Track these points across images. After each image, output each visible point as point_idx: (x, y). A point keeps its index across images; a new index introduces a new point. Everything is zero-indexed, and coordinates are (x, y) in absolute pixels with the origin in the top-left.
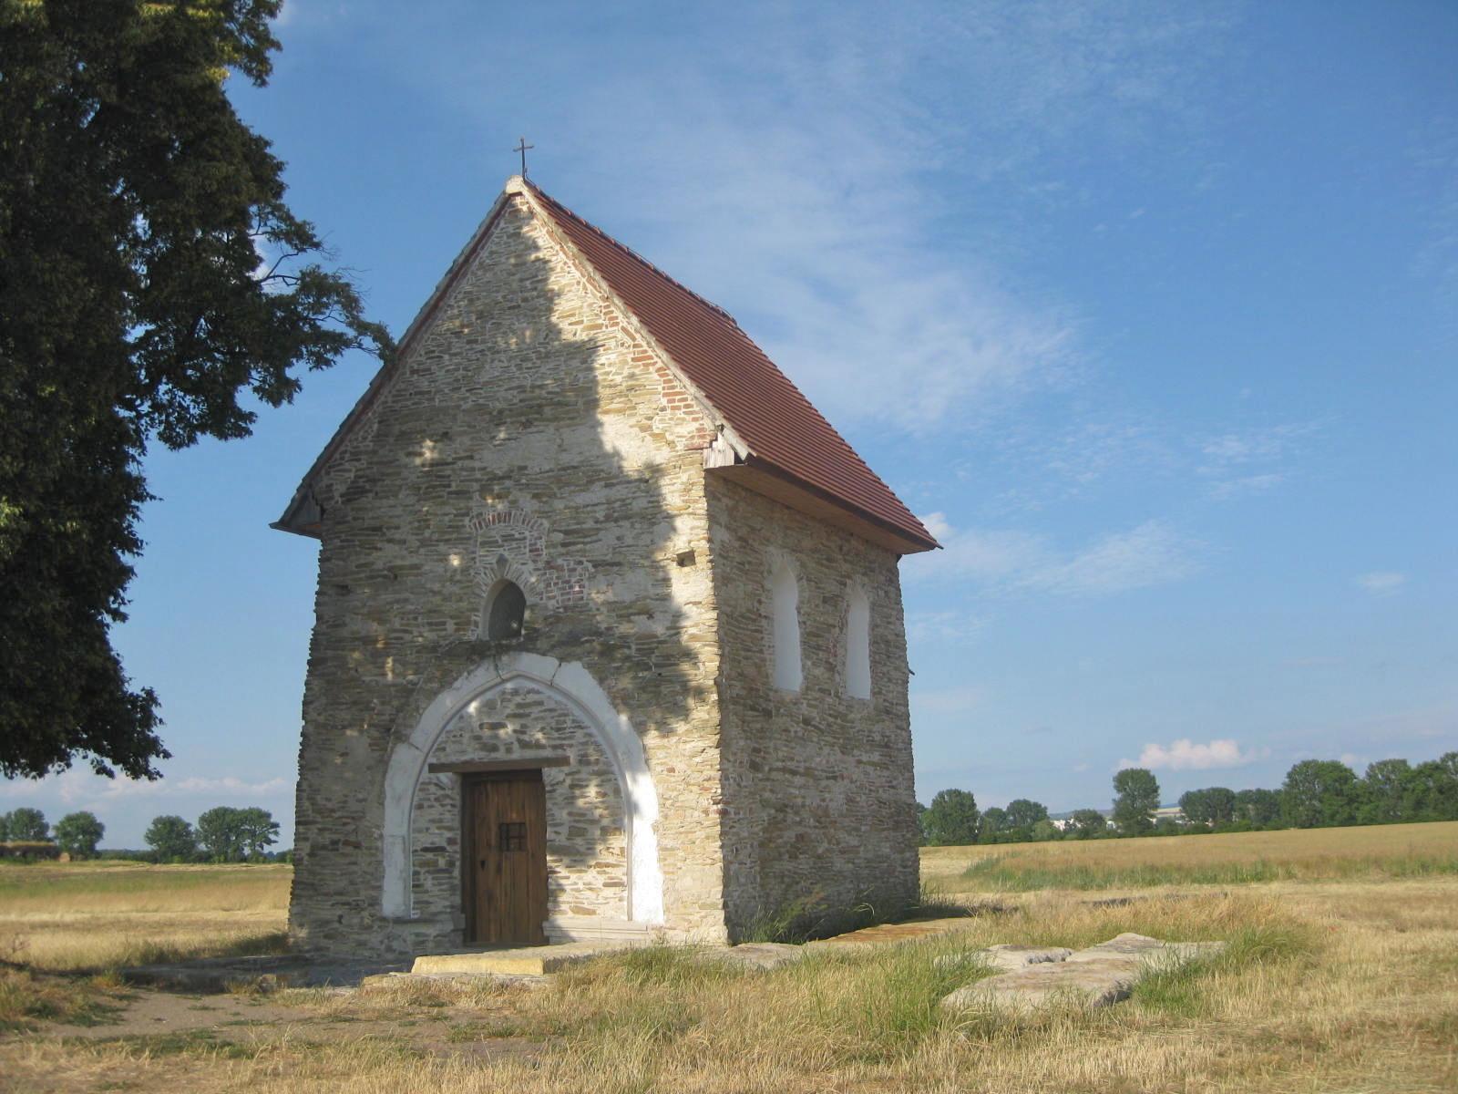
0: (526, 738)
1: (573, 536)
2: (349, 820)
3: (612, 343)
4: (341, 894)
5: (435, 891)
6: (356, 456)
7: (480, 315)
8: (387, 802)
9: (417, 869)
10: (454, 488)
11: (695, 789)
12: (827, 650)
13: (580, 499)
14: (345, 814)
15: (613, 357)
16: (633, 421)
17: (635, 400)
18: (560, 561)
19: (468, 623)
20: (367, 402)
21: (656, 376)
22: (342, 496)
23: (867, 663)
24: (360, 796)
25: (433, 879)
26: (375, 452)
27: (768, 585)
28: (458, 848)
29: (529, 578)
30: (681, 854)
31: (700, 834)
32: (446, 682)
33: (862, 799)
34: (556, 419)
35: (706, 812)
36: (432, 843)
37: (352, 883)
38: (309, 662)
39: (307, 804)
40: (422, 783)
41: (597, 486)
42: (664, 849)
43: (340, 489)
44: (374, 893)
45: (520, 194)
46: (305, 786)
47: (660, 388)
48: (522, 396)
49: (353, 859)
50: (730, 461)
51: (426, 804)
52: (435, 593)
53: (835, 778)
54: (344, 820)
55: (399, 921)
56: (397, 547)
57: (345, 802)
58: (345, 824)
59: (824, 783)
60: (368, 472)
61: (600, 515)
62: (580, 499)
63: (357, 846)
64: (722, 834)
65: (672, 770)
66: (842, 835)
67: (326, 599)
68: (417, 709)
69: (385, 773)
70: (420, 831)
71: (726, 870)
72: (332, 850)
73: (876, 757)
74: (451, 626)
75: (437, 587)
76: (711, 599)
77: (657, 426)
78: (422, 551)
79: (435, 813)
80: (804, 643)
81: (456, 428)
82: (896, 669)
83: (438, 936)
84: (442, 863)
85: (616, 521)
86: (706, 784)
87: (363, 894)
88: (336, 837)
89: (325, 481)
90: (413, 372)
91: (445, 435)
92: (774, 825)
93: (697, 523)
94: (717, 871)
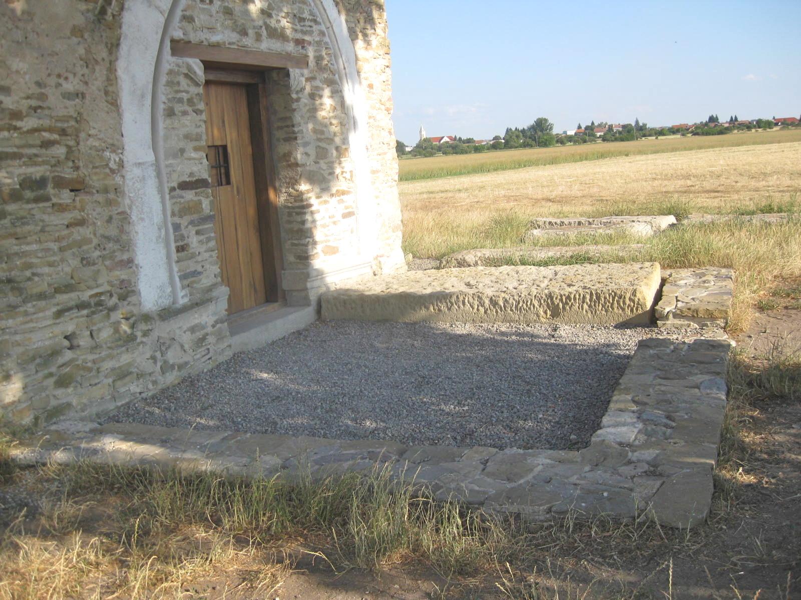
0: (272, 23)
2: (55, 137)
4: (68, 288)
9: (177, 220)
14: (46, 123)
24: (69, 86)
25: (198, 233)
36: (191, 174)
37: (86, 262)
40: (170, 72)
44: (122, 274)
49: (76, 214)
51: (178, 108)
54: (46, 135)
55: (168, 313)
57: (42, 97)
58: (47, 144)
69: (114, 46)
72: (37, 200)
83: (216, 322)
88: (37, 172)
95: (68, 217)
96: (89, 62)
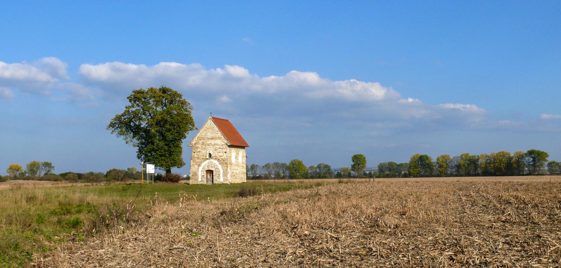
1: (216, 150)
6: (195, 141)
13: (217, 146)
29: (211, 153)
32: (204, 161)
33: (240, 171)
42: (223, 176)
43: (194, 143)
62: (217, 146)
74: (205, 157)
92: (232, 174)
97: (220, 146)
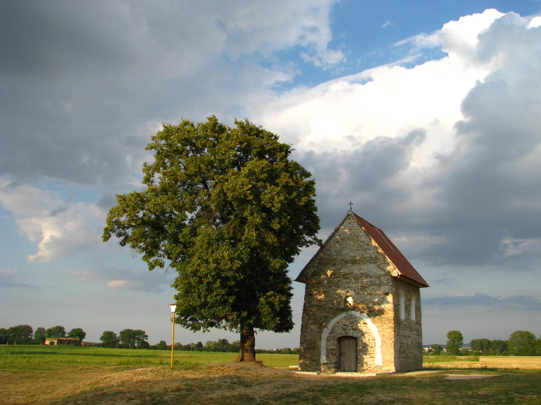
0: (353, 328)
3: (372, 249)
5: (333, 358)
6: (314, 267)
7: (342, 240)
8: (322, 340)
10: (336, 276)
11: (389, 339)
12: (408, 310)
15: (372, 252)
16: (376, 265)
17: (377, 261)
18: (360, 293)
19: (340, 304)
20: (316, 256)
21: (381, 256)
22: (310, 275)
23: (414, 313)
24: (315, 338)
26: (318, 267)
27: (400, 298)
28: (337, 349)
30: (386, 352)
31: (390, 348)
32: (335, 315)
33: (413, 342)
34: (359, 263)
35: (391, 344)
37: (314, 356)
38: (303, 310)
39: (303, 340)
41: (368, 278)
43: (310, 274)
45: (351, 215)
46: (302, 335)
47: (382, 259)
48: (352, 258)
50: (397, 275)
51: (331, 340)
52: (333, 297)
53: (409, 337)
56: (323, 287)
58: (312, 344)
59: (408, 338)
60: (316, 271)
61: (369, 284)
63: (315, 348)
64: (394, 348)
65: (384, 336)
66: (410, 349)
67: (307, 297)
68: (329, 321)
69: (321, 334)
70: (329, 346)
71: (394, 355)
73: (416, 333)
75: (333, 296)
76: (392, 302)
77: (381, 267)
78: (329, 288)
79: (333, 342)
80: (405, 309)
81: (337, 263)
82: (420, 313)
84: (334, 352)
85: (372, 285)
86: (391, 339)
87: (316, 358)
88: (310, 346)
89: (307, 272)
90: (326, 250)
91: (334, 264)
92: (401, 347)
93: (390, 287)
94: (393, 356)
95: (312, 351)
96: (318, 335)
97: (373, 279)
